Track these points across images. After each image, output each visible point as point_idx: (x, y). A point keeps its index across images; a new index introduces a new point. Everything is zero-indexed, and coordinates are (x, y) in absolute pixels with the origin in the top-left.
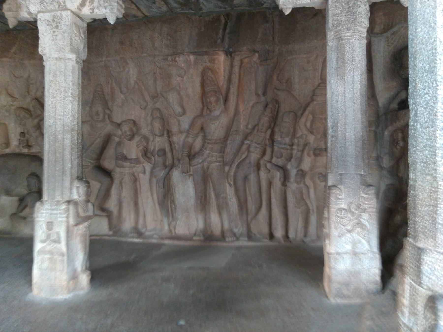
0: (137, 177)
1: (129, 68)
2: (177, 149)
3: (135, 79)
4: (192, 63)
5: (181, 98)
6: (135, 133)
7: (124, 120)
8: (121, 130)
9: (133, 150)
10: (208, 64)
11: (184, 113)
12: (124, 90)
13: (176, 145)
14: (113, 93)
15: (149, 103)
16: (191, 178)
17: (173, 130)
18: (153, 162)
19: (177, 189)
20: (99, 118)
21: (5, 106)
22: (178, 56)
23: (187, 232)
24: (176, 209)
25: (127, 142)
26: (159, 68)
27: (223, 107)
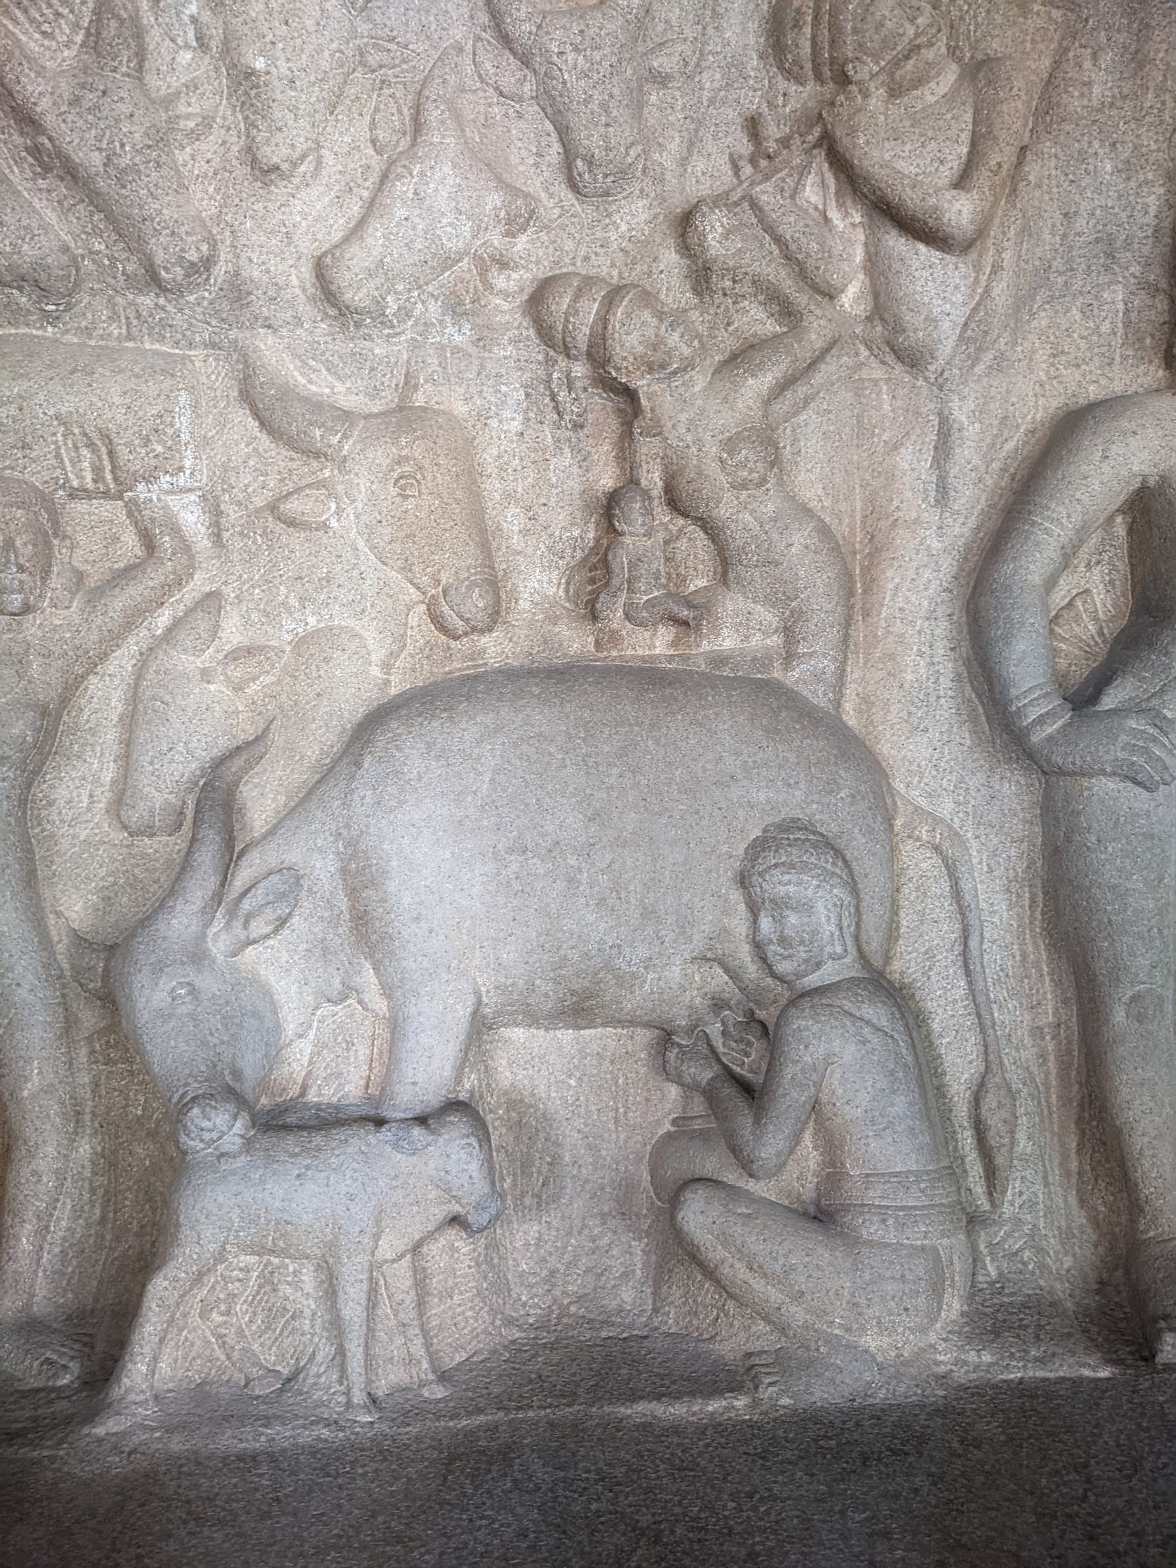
21: (449, 262)
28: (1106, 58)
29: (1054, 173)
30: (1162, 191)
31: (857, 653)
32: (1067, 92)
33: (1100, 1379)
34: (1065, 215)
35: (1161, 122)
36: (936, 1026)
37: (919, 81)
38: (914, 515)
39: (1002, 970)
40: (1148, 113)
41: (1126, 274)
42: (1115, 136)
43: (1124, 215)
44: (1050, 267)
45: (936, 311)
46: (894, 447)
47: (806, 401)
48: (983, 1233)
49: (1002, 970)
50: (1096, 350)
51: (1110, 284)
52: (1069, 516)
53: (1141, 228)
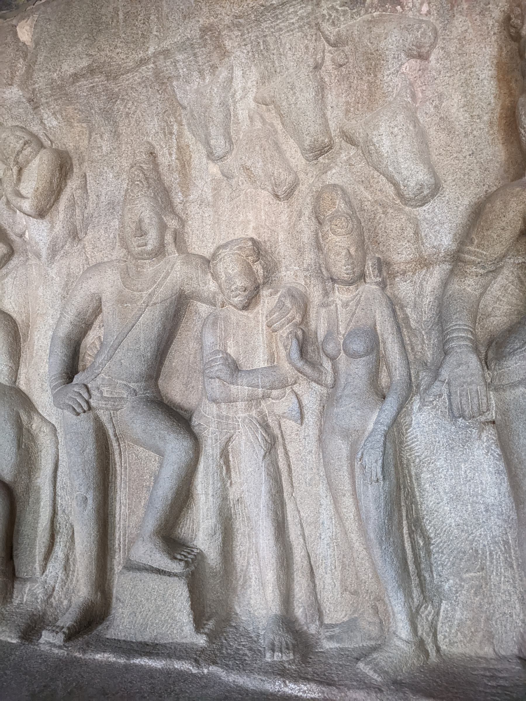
0: (277, 432)
1: (231, 69)
2: (413, 324)
3: (253, 105)
5: (422, 136)
6: (261, 281)
7: (222, 242)
8: (215, 277)
9: (257, 338)
11: (436, 189)
12: (219, 143)
13: (408, 310)
15: (302, 176)
16: (489, 433)
17: (395, 258)
18: (329, 380)
19: (425, 476)
20: (146, 245)
23: (487, 651)
24: (429, 553)
25: (236, 315)
26: (334, 45)
28: (106, 136)
29: (91, 182)
31: (25, 364)
33: (12, 643)
34: (97, 196)
36: (42, 504)
37: (28, 162)
38: (45, 312)
39: (65, 484)
40: (123, 153)
43: (117, 193)
44: (92, 216)
45: (37, 240)
46: (37, 288)
47: (7, 274)
48: (29, 585)
49: (65, 484)
51: (113, 219)
52: (71, 311)
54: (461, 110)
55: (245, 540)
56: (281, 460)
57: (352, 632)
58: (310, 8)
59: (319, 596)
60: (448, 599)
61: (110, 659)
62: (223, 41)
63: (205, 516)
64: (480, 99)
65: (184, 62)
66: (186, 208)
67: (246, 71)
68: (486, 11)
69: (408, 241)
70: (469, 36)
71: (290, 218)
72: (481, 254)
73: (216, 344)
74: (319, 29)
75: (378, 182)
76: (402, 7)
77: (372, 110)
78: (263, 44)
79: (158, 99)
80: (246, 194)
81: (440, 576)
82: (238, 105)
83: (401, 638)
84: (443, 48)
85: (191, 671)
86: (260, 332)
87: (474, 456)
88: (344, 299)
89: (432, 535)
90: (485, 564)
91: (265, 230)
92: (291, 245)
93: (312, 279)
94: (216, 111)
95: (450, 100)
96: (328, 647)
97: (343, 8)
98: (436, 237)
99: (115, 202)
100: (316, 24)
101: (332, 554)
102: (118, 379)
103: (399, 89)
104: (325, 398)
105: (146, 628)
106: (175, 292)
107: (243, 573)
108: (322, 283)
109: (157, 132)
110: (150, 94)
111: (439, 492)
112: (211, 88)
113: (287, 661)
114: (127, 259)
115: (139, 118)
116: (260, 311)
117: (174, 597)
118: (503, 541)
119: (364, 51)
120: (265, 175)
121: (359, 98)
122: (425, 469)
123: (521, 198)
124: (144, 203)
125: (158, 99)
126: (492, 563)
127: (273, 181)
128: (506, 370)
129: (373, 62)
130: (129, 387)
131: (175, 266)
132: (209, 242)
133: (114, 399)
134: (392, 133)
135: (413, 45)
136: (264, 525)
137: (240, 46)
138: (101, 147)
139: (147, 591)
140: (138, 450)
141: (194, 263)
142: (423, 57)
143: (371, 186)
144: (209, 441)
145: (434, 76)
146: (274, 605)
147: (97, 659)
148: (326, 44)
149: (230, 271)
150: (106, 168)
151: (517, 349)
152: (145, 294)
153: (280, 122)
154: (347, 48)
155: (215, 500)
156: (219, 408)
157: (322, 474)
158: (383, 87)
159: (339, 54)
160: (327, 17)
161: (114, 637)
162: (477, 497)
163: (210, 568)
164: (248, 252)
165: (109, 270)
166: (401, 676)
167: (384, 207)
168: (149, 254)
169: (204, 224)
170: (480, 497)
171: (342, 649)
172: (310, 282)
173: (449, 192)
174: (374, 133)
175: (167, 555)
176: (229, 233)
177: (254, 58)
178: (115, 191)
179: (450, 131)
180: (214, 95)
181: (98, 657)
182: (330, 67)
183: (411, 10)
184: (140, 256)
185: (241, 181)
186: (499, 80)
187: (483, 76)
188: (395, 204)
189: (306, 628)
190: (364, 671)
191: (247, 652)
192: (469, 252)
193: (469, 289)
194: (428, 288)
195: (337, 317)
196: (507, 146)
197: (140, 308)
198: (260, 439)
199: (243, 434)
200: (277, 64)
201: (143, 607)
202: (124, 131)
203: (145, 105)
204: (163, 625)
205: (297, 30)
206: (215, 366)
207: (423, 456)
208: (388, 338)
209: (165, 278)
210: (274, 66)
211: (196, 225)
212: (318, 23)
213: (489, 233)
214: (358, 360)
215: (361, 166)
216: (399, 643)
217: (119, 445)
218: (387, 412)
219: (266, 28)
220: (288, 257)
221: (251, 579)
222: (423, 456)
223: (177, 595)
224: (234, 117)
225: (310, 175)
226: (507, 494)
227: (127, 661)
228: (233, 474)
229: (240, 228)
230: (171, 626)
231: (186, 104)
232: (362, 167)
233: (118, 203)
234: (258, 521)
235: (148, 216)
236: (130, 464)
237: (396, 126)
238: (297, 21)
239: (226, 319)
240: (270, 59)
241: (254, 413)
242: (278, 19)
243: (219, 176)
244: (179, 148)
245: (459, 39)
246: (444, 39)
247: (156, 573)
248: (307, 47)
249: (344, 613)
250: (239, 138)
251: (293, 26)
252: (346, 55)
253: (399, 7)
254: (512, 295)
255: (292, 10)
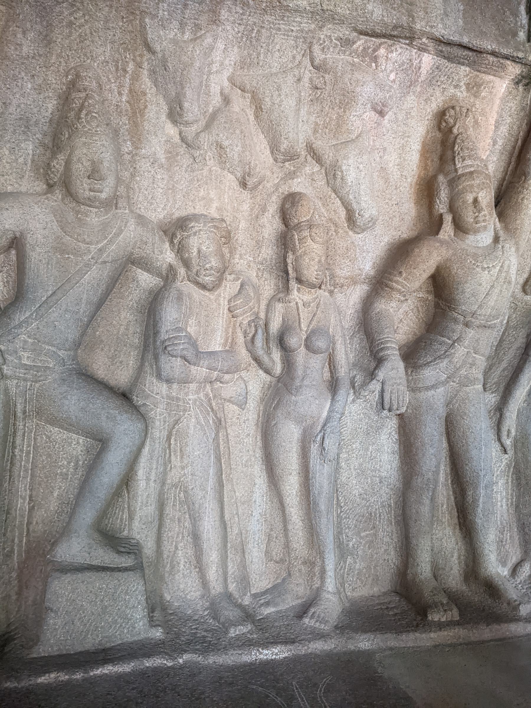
0: (220, 415)
1: (215, 39)
3: (226, 83)
4: (422, 78)
10: (462, 94)
14: (137, 111)
18: (278, 369)
20: (101, 192)
22: (390, 42)
27: (498, 225)
28: (31, 35)
30: (55, 102)
32: (7, 46)
34: (4, 103)
35: (59, 71)
40: (52, 65)
41: (34, 137)
42: (33, 72)
43: (35, 110)
50: (14, 170)
51: (25, 140)
53: (44, 117)
54: (396, 167)
55: (175, 525)
56: (222, 443)
57: (284, 595)
58: (313, 26)
59: (248, 570)
60: (352, 554)
61: (60, 679)
62: (220, 9)
63: (144, 502)
64: (409, 164)
65: (168, 5)
66: (135, 161)
67: (228, 47)
68: (429, 100)
69: (350, 261)
70: (413, 114)
71: (252, 210)
72: (406, 285)
73: (179, 321)
74: (310, 48)
75: (333, 203)
76: (376, 66)
77: (338, 139)
78: (257, 33)
79: (119, 26)
80: (210, 171)
81: (348, 536)
82: (211, 76)
83: (329, 591)
84: (395, 114)
85: (166, 664)
86: (221, 315)
87: (380, 440)
88: (305, 300)
89: (342, 504)
90: (376, 523)
91: (229, 214)
92: (250, 235)
93: (265, 273)
94: (194, 74)
95: (389, 156)
96: (266, 613)
97: (336, 42)
98: (363, 261)
99: (30, 120)
100: (310, 42)
101: (260, 529)
102: (48, 344)
103: (360, 131)
104: (267, 386)
105: (88, 634)
106: (126, 253)
107: (170, 559)
108: (276, 279)
109: (107, 62)
110: (111, 16)
111: (350, 469)
112: (193, 47)
113: (248, 632)
114: (58, 198)
115: (86, 35)
116: (222, 294)
117: (127, 593)
118: (388, 504)
119: (343, 87)
120: (240, 161)
121: (327, 124)
122: (344, 450)
123: (440, 251)
124: (104, 142)
125: (119, 26)
126: (380, 522)
127: (248, 170)
128: (421, 376)
129: (347, 100)
130: (59, 356)
131: (128, 224)
132: (159, 207)
133: (38, 369)
134: (358, 167)
135: (380, 102)
136: (211, 507)
137: (234, 22)
138: (21, 45)
139: (91, 592)
140: (51, 431)
141: (150, 227)
142: (381, 114)
143: (328, 205)
144: (157, 423)
145: (384, 132)
146: (218, 584)
147: (42, 683)
148: (309, 63)
149: (204, 248)
150: (23, 74)
151: (431, 362)
152: (93, 248)
153: (252, 113)
154: (327, 76)
155: (156, 486)
156: (170, 388)
157: (257, 456)
158: (348, 124)
159: (319, 78)
160: (321, 42)
161: (43, 655)
162: (375, 472)
163: (148, 557)
164: (224, 233)
165: (36, 206)
166: (335, 622)
167: (336, 226)
168: (101, 203)
169: (156, 186)
170: (377, 472)
171: (278, 612)
172: (262, 275)
173: (379, 229)
174: (345, 162)
175: (112, 550)
176: (186, 205)
177: (242, 40)
178: (32, 107)
179: (387, 180)
180: (196, 57)
181: (41, 680)
182: (307, 85)
183: (382, 71)
184: (90, 202)
185: (209, 156)
186: (421, 155)
187: (414, 147)
188: (344, 227)
189: (240, 601)
190: (310, 624)
191: (205, 634)
192: (397, 282)
193: (391, 310)
194: (352, 303)
195: (299, 315)
196: (417, 206)
197: (88, 264)
198: (211, 422)
199: (193, 417)
200: (262, 57)
201: (83, 612)
202: (59, 40)
203: (100, 25)
204: (111, 627)
205: (292, 38)
206: (179, 344)
207: (346, 440)
208: (338, 340)
209: (117, 235)
210: (258, 58)
211: (146, 184)
212: (312, 43)
213: (415, 271)
214: (318, 356)
215: (321, 182)
216: (329, 596)
217: (25, 425)
218: (340, 403)
219: (268, 21)
220: (245, 246)
221: (179, 563)
222: (346, 440)
223: (131, 591)
224: (206, 87)
225: (275, 175)
226: (396, 469)
227: (86, 675)
228: (173, 458)
229: (201, 203)
230: (121, 626)
231: (158, 49)
232: (322, 185)
233: (36, 123)
234: (203, 504)
235: (108, 159)
236: (35, 448)
237: (361, 163)
238: (297, 31)
239: (190, 296)
240: (257, 49)
241: (201, 395)
242: (283, 19)
243: (177, 139)
244: (130, 91)
245: (406, 112)
246: (398, 107)
247: (103, 571)
248: (294, 57)
249: (268, 581)
250: (208, 111)
251: (291, 33)
252: (325, 82)
253: (374, 65)
254: (411, 320)
255: (298, 19)
